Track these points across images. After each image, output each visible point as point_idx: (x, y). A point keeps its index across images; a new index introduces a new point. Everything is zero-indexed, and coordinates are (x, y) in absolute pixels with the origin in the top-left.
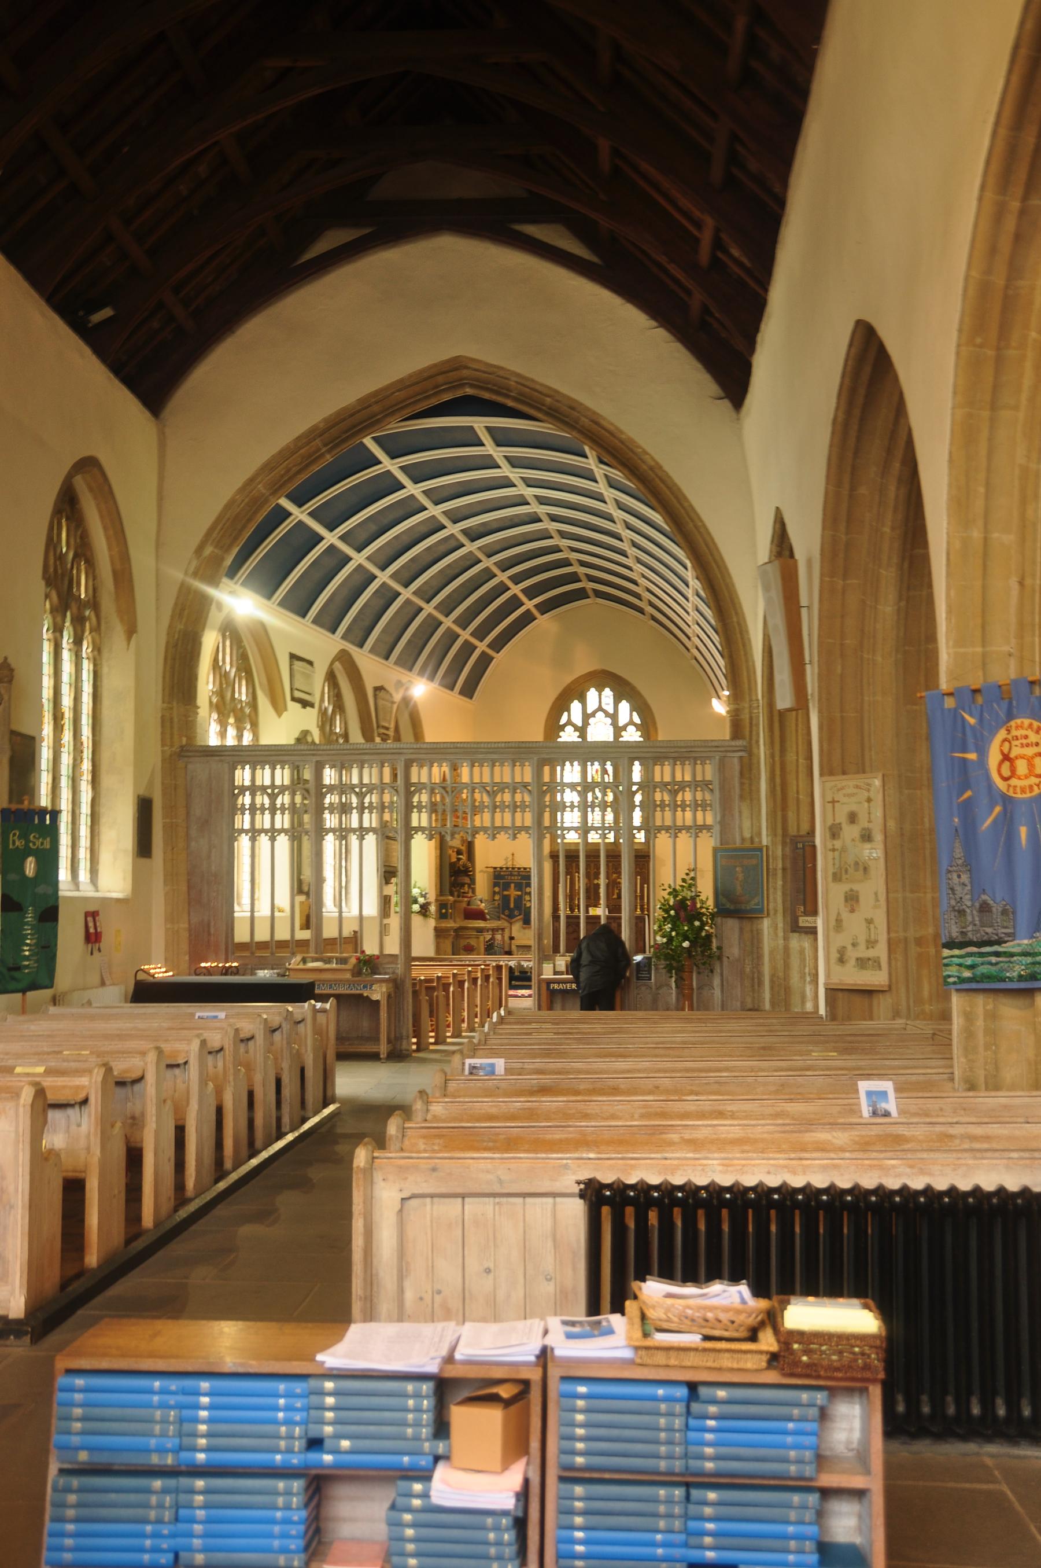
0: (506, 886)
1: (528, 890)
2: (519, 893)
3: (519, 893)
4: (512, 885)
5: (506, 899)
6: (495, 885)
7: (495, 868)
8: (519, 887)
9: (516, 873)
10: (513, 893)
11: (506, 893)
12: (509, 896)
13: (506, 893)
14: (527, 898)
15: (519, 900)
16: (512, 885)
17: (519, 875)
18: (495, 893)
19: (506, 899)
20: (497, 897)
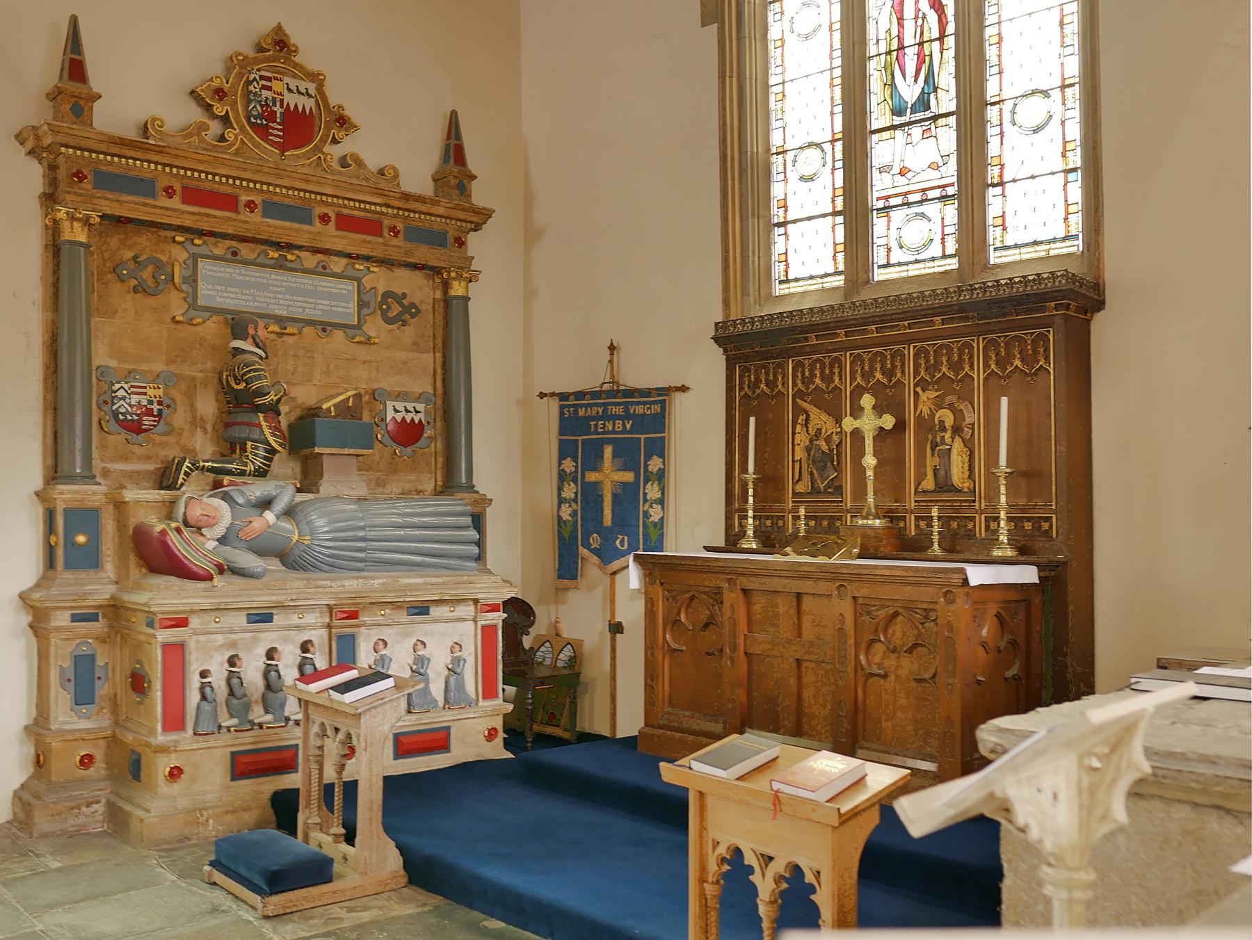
0: (593, 460)
1: (655, 464)
2: (629, 477)
3: (629, 477)
4: (608, 451)
5: (591, 496)
6: (566, 450)
7: (563, 397)
8: (628, 456)
9: (619, 410)
10: (610, 475)
11: (592, 477)
12: (596, 484)
13: (592, 477)
14: (653, 491)
15: (628, 497)
16: (608, 451)
17: (626, 416)
18: (562, 477)
19: (591, 496)
20: (569, 491)
